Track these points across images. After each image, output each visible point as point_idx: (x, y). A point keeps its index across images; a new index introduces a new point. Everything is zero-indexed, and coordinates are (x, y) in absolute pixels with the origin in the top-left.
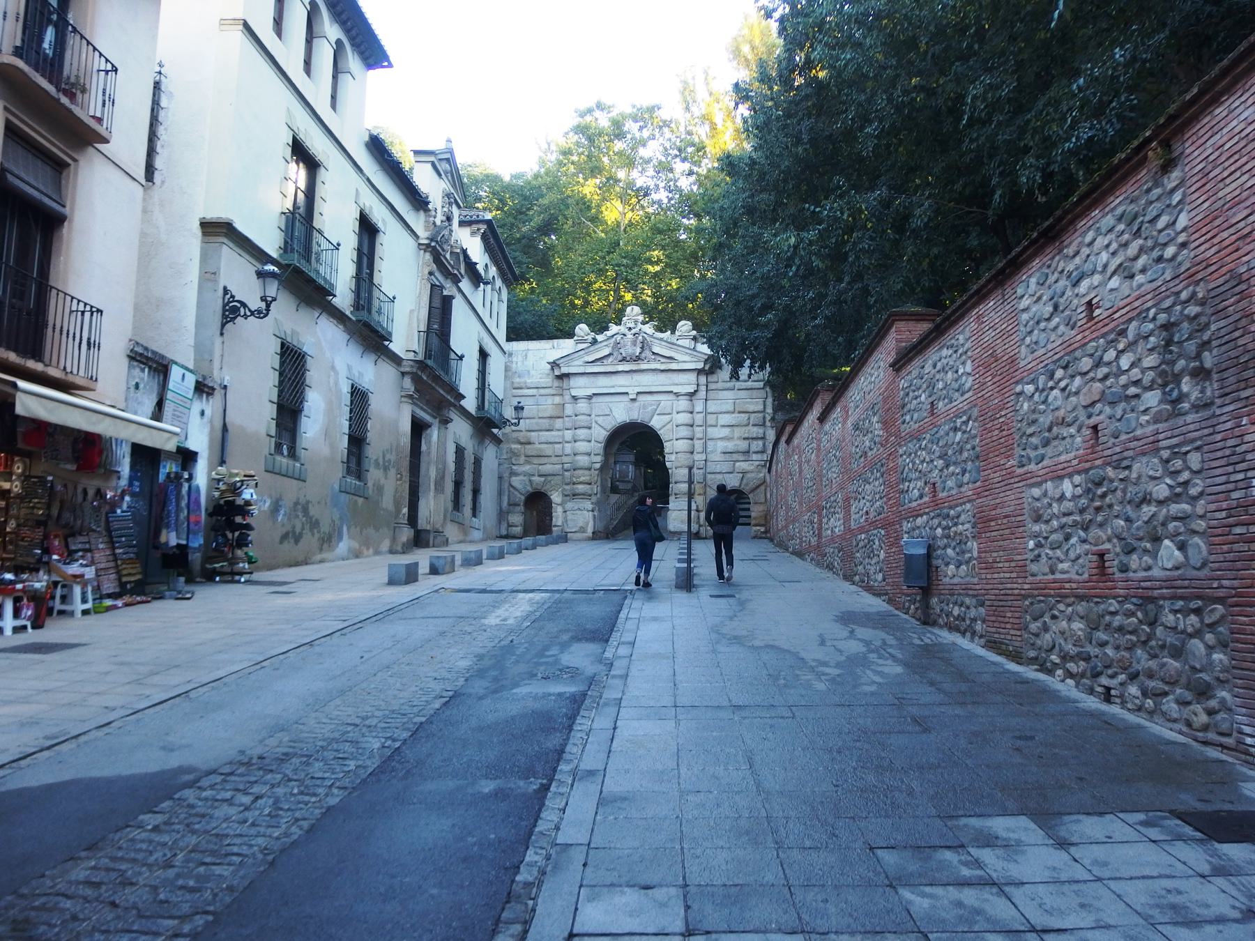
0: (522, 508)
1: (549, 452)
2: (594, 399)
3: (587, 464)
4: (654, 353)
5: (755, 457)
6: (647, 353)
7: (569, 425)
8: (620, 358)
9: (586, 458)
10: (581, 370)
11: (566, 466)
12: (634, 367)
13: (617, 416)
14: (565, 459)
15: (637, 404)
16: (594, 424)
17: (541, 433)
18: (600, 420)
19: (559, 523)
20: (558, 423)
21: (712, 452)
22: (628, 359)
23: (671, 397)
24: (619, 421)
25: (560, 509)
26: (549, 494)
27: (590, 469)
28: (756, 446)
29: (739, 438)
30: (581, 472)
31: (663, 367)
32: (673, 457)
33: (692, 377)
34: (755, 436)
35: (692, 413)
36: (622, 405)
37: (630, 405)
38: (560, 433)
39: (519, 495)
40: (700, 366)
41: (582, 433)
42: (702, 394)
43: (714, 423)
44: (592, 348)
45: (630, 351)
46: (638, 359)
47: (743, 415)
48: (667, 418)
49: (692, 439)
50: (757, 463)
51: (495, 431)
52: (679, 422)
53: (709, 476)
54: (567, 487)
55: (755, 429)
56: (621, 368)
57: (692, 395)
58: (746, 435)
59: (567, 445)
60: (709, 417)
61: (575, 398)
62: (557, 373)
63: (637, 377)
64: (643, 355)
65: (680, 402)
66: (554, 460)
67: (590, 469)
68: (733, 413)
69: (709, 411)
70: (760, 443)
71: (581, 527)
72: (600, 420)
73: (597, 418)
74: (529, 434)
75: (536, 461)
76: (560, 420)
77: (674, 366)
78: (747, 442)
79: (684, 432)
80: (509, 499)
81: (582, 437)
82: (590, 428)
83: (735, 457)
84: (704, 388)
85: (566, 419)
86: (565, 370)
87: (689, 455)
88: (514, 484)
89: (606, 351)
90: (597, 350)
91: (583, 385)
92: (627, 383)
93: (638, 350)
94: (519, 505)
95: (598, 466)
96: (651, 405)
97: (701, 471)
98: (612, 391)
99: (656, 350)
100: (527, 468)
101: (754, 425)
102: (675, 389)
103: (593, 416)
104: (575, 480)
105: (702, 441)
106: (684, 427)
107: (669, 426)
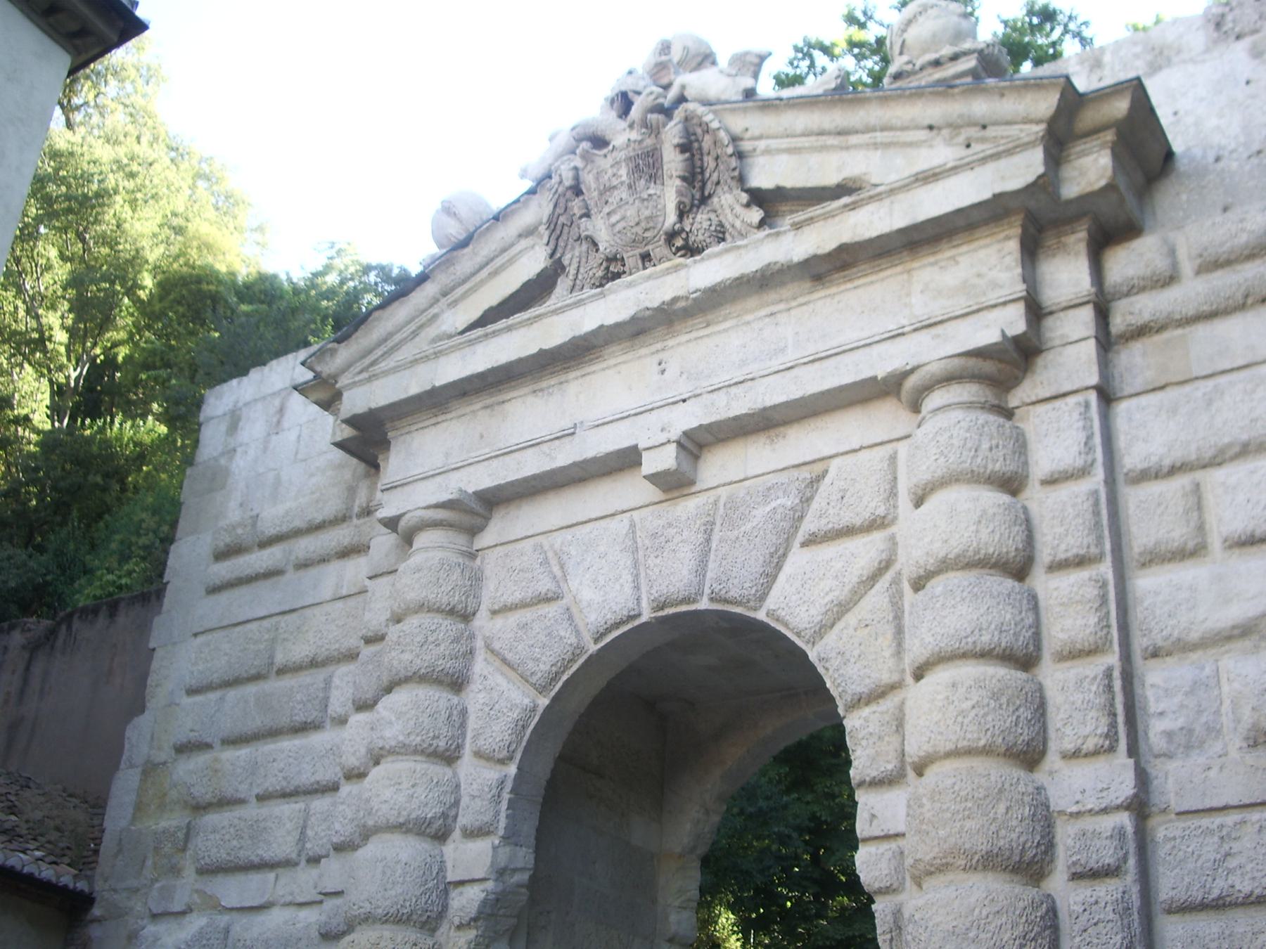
1: (281, 844)
2: (499, 529)
4: (758, 198)
6: (729, 203)
9: (407, 849)
15: (689, 507)
16: (480, 666)
17: (268, 747)
21: (1187, 741)
36: (619, 526)
48: (865, 551)
60: (1135, 498)
69: (1133, 457)
84: (1080, 323)
89: (532, 263)
96: (767, 493)
97: (1106, 890)
98: (564, 456)
102: (882, 362)
105: (1094, 667)
106: (954, 579)
107: (877, 598)
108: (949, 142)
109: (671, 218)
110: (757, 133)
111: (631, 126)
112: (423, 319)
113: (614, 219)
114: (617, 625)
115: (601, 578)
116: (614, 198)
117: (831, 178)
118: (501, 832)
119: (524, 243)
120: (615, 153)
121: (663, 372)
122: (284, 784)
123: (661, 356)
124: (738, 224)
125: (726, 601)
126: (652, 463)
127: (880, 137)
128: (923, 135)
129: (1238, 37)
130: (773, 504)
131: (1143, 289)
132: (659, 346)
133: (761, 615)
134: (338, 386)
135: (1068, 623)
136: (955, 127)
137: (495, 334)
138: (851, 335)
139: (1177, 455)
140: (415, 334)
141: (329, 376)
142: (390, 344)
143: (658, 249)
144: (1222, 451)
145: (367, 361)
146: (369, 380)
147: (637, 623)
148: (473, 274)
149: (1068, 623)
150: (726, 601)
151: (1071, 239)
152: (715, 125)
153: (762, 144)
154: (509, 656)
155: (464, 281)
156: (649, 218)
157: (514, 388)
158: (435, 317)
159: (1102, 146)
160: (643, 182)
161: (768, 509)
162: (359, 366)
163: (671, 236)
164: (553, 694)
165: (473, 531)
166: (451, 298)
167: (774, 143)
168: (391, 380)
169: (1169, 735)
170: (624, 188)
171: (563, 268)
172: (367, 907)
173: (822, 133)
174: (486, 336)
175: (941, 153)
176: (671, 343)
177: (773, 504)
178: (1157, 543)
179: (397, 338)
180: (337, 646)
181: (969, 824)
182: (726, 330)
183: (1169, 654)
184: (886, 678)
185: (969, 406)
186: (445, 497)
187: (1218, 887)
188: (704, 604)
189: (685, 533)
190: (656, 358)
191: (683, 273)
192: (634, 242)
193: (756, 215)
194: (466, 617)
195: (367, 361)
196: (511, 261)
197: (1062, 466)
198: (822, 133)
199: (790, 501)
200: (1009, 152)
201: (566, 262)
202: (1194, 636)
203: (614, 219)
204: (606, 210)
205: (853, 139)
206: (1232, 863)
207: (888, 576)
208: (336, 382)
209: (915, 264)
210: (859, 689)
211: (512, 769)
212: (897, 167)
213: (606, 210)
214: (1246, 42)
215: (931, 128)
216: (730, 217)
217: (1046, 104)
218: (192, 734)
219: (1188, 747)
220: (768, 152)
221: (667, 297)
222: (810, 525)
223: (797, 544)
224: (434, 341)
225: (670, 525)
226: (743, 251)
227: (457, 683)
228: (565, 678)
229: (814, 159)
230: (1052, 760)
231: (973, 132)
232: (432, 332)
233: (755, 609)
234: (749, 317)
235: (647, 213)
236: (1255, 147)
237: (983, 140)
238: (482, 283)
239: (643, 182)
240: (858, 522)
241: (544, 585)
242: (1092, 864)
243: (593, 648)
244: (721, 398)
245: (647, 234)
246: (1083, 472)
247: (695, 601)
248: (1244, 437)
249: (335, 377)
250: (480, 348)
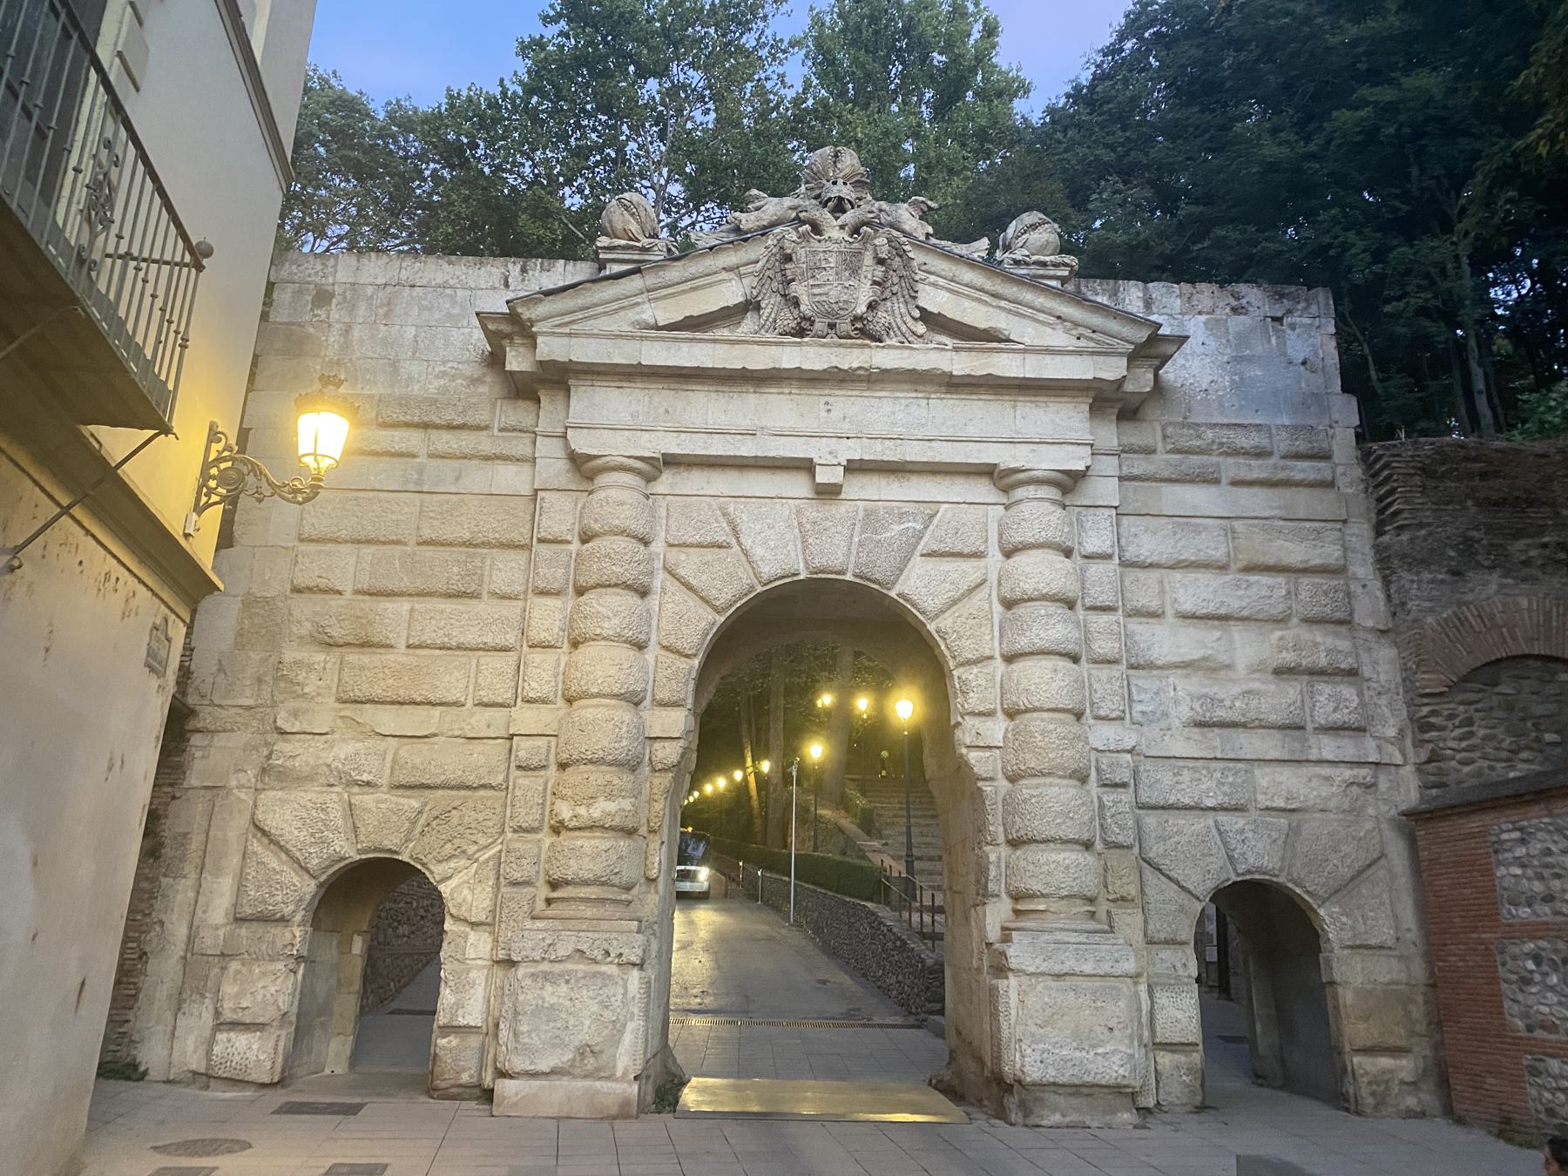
0: (296, 935)
2: (667, 482)
3: (623, 747)
4: (926, 316)
5: (1328, 747)
7: (553, 574)
8: (788, 319)
9: (624, 714)
10: (621, 354)
11: (524, 748)
12: (853, 358)
13: (758, 552)
14: (526, 719)
16: (659, 580)
18: (688, 562)
19: (473, 1014)
20: (506, 571)
21: (1148, 719)
22: (820, 326)
23: (982, 490)
24: (767, 570)
25: (478, 946)
26: (435, 872)
27: (630, 765)
28: (1331, 702)
29: (1256, 669)
30: (599, 776)
31: (963, 363)
32: (996, 730)
33: (1070, 418)
34: (1323, 661)
35: (1068, 553)
36: (784, 510)
37: (813, 512)
38: (512, 610)
39: (292, 877)
40: (1113, 369)
41: (611, 609)
42: (1105, 489)
43: (1154, 604)
44: (675, 272)
45: (834, 293)
46: (865, 331)
47: (1266, 579)
48: (968, 571)
49: (1075, 659)
50: (1348, 773)
51: (114, 441)
52: (1028, 586)
53: (1151, 820)
54: (524, 845)
55: (1318, 635)
56: (792, 356)
57: (1068, 483)
58: (1289, 658)
59: (537, 656)
61: (584, 468)
62: (517, 361)
63: (848, 406)
64: (882, 317)
65: (1026, 509)
66: (480, 721)
67: (630, 765)
68: (1223, 568)
70: (1348, 692)
71: (584, 1051)
72: (688, 562)
73: (673, 555)
74: (367, 603)
75: (388, 720)
76: (519, 558)
77: (1007, 365)
78: (1292, 691)
79: (1051, 628)
80: (240, 889)
81: (609, 627)
82: (643, 593)
83: (1252, 744)
85: (544, 550)
86: (551, 348)
87: (1070, 727)
88: (271, 822)
89: (731, 293)
90: (692, 284)
91: (624, 418)
92: (808, 425)
93: (864, 294)
94: (284, 921)
95: (669, 753)
96: (902, 516)
97: (1126, 796)
98: (747, 449)
99: (934, 299)
100: (343, 751)
101: (1310, 621)
103: (658, 547)
104: (565, 811)
106: (1052, 608)
108: (1067, 331)
109: (861, 309)
110: (933, 269)
111: (842, 227)
112: (626, 303)
113: (816, 291)
114: (783, 577)
115: (771, 543)
116: (822, 276)
117: (982, 324)
118: (689, 706)
119: (724, 275)
120: (829, 244)
121: (829, 411)
122: (446, 640)
123: (831, 400)
124: (904, 328)
125: (869, 580)
126: (823, 476)
127: (1022, 310)
128: (1052, 320)
129: (1200, 313)
130: (907, 525)
131: (1135, 452)
132: (827, 392)
133: (893, 594)
134: (534, 329)
135: (1103, 644)
136: (1076, 324)
137: (701, 341)
138: (972, 431)
139: (1155, 559)
140: (616, 311)
141: (529, 320)
142: (591, 312)
143: (845, 326)
144: (1180, 562)
145: (567, 319)
146: (569, 335)
147: (795, 578)
148: (678, 283)
149: (1103, 644)
150: (869, 580)
151: (1109, 410)
152: (911, 255)
153: (932, 278)
154: (694, 582)
155: (669, 286)
156: (846, 302)
157: (699, 383)
158: (638, 304)
159: (1150, 366)
160: (847, 273)
161: (903, 527)
162: (558, 321)
163: (857, 319)
164: (728, 614)
165: (649, 479)
166: (653, 295)
167: (941, 282)
168: (593, 344)
169: (1143, 713)
170: (832, 272)
171: (757, 307)
172: (601, 753)
173: (981, 290)
174: (693, 340)
175: (1059, 338)
176: (837, 392)
177: (907, 525)
178: (1143, 606)
179: (600, 309)
180: (497, 535)
181: (1066, 753)
182: (880, 398)
183: (1143, 668)
184: (987, 653)
185: (1054, 502)
186: (647, 454)
187: (1172, 799)
188: (849, 577)
189: (839, 528)
190: (823, 400)
191: (867, 350)
192: (828, 314)
193: (921, 328)
194: (646, 542)
195: (567, 319)
196: (710, 285)
197: (1100, 551)
198: (981, 290)
199: (918, 527)
200: (1106, 354)
201: (763, 305)
202: (1160, 663)
203: (816, 291)
204: (811, 282)
205: (1003, 303)
206: (1179, 787)
207: (985, 589)
208: (532, 326)
209: (1021, 398)
210: (970, 656)
211: (696, 662)
212: (1024, 331)
213: (811, 282)
214: (1203, 318)
215: (1059, 317)
216: (898, 320)
217: (1142, 335)
218: (319, 580)
219: (1152, 721)
220: (934, 285)
221: (855, 365)
222: (927, 544)
223: (917, 553)
224: (632, 324)
225: (827, 519)
226: (915, 353)
227: (643, 593)
228: (738, 605)
229: (967, 303)
230: (1088, 718)
231: (1088, 332)
232: (631, 315)
233: (889, 589)
234: (899, 394)
235: (845, 297)
236: (1204, 386)
237: (1091, 339)
238: (684, 292)
239: (847, 273)
240: (966, 551)
241: (721, 539)
242: (1117, 780)
243: (760, 589)
244: (878, 445)
245: (841, 312)
246: (1109, 557)
247: (844, 574)
248: (1193, 558)
249: (532, 322)
250: (685, 346)
